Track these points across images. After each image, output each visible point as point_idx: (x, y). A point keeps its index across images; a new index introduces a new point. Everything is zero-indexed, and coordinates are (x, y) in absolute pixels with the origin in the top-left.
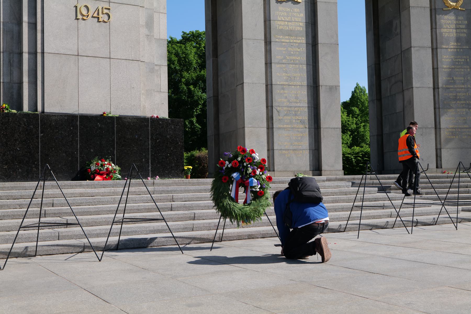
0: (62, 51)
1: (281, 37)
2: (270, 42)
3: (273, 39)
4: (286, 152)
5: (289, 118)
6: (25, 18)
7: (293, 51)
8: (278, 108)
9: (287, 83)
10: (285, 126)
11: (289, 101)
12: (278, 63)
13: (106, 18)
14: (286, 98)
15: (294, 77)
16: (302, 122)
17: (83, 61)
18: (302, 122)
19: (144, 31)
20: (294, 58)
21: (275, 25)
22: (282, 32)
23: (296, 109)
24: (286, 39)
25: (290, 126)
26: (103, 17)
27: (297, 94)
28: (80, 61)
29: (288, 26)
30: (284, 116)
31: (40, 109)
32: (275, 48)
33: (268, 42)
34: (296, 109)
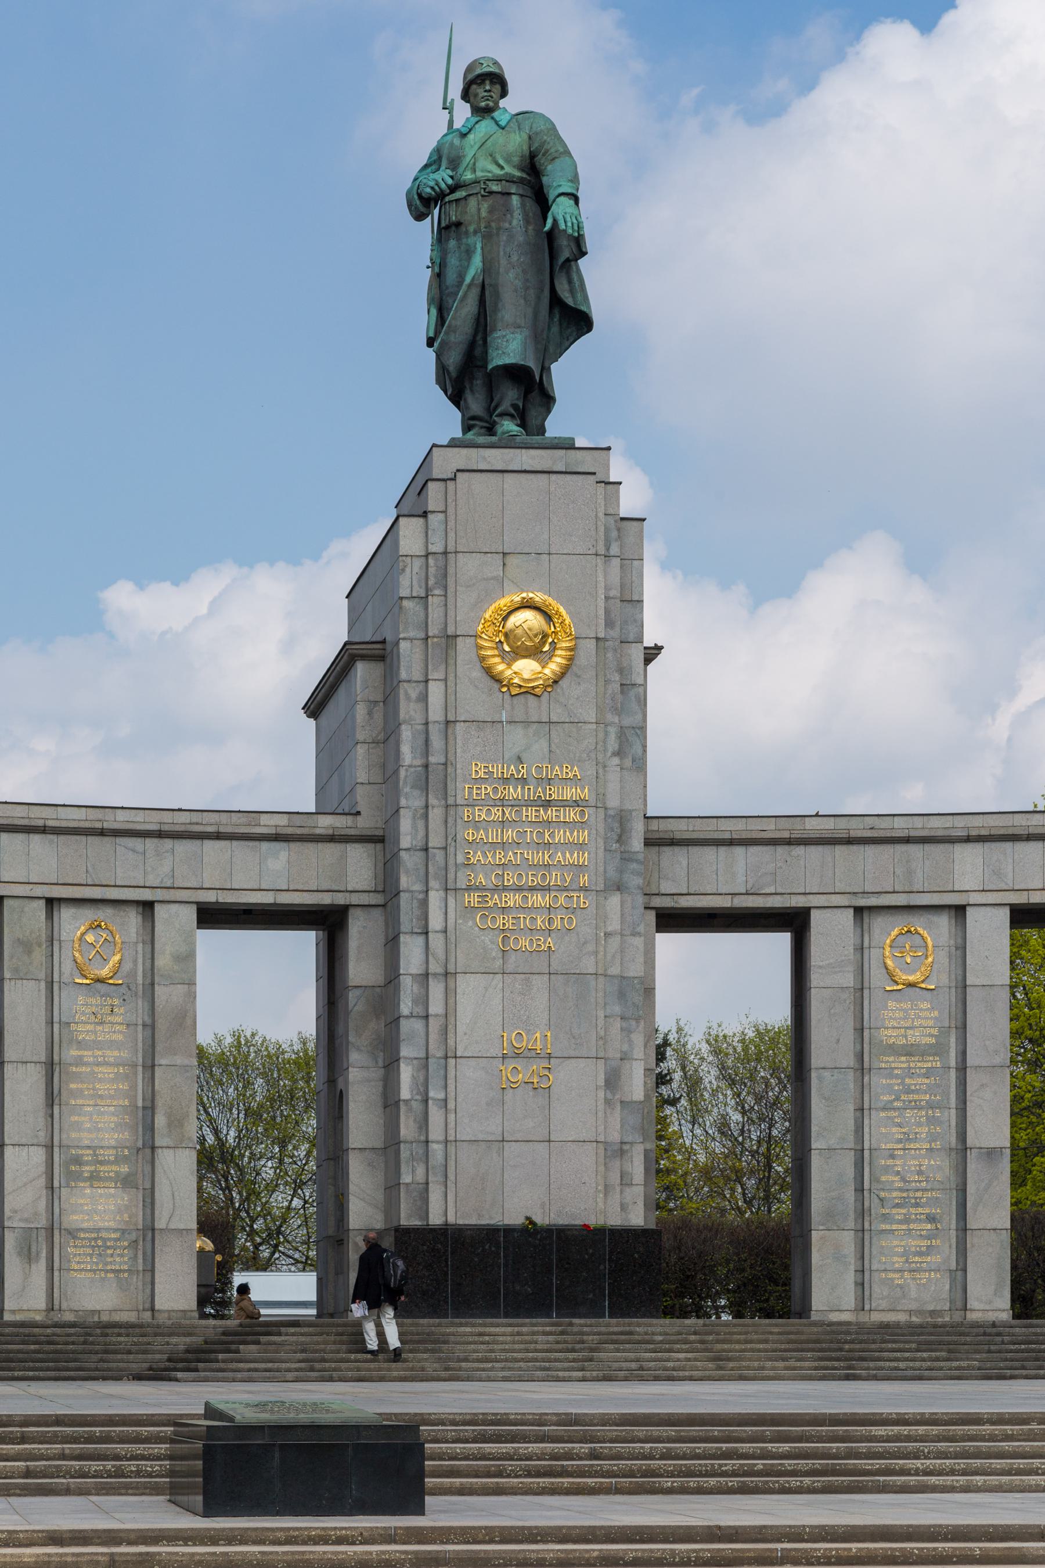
0: (481, 1137)
1: (891, 1059)
4: (897, 1276)
5: (904, 1211)
7: (915, 1085)
8: (882, 1194)
9: (900, 1146)
10: (894, 1227)
12: (884, 1109)
14: (898, 1173)
15: (916, 1133)
16: (931, 1219)
17: (510, 1149)
20: (916, 1097)
22: (894, 1050)
24: (901, 1063)
27: (920, 1165)
28: (506, 1148)
30: (894, 1207)
32: (878, 1081)
33: (861, 1069)
34: (919, 1194)
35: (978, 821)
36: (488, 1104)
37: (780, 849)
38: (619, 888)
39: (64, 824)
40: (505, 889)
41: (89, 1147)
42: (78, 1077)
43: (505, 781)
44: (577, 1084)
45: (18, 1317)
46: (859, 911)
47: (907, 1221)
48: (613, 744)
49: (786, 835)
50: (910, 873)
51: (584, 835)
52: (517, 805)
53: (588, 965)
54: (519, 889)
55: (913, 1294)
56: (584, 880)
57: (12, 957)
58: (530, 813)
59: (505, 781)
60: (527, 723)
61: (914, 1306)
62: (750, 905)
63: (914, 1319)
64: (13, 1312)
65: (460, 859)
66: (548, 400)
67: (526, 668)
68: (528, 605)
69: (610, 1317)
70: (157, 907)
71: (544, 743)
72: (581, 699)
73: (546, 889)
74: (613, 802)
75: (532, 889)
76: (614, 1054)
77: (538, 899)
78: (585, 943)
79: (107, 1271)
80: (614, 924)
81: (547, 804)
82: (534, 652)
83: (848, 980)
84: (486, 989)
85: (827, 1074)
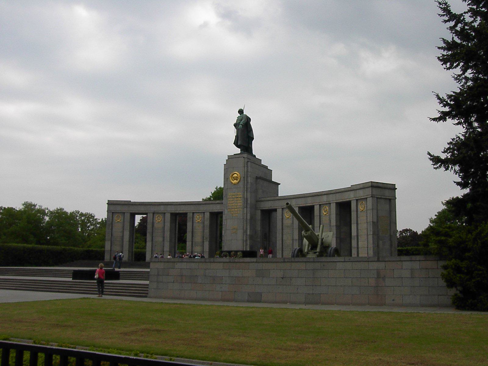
16: (290, 249)
38: (247, 207)
40: (232, 209)
43: (233, 195)
44: (240, 233)
48: (245, 190)
51: (241, 201)
52: (234, 198)
54: (234, 208)
56: (241, 207)
58: (235, 199)
59: (233, 195)
60: (235, 188)
67: (235, 181)
68: (235, 174)
70: (205, 213)
72: (241, 184)
73: (237, 208)
74: (245, 197)
75: (236, 208)
76: (245, 228)
77: (236, 210)
80: (245, 212)
81: (237, 198)
82: (236, 179)
83: (281, 218)
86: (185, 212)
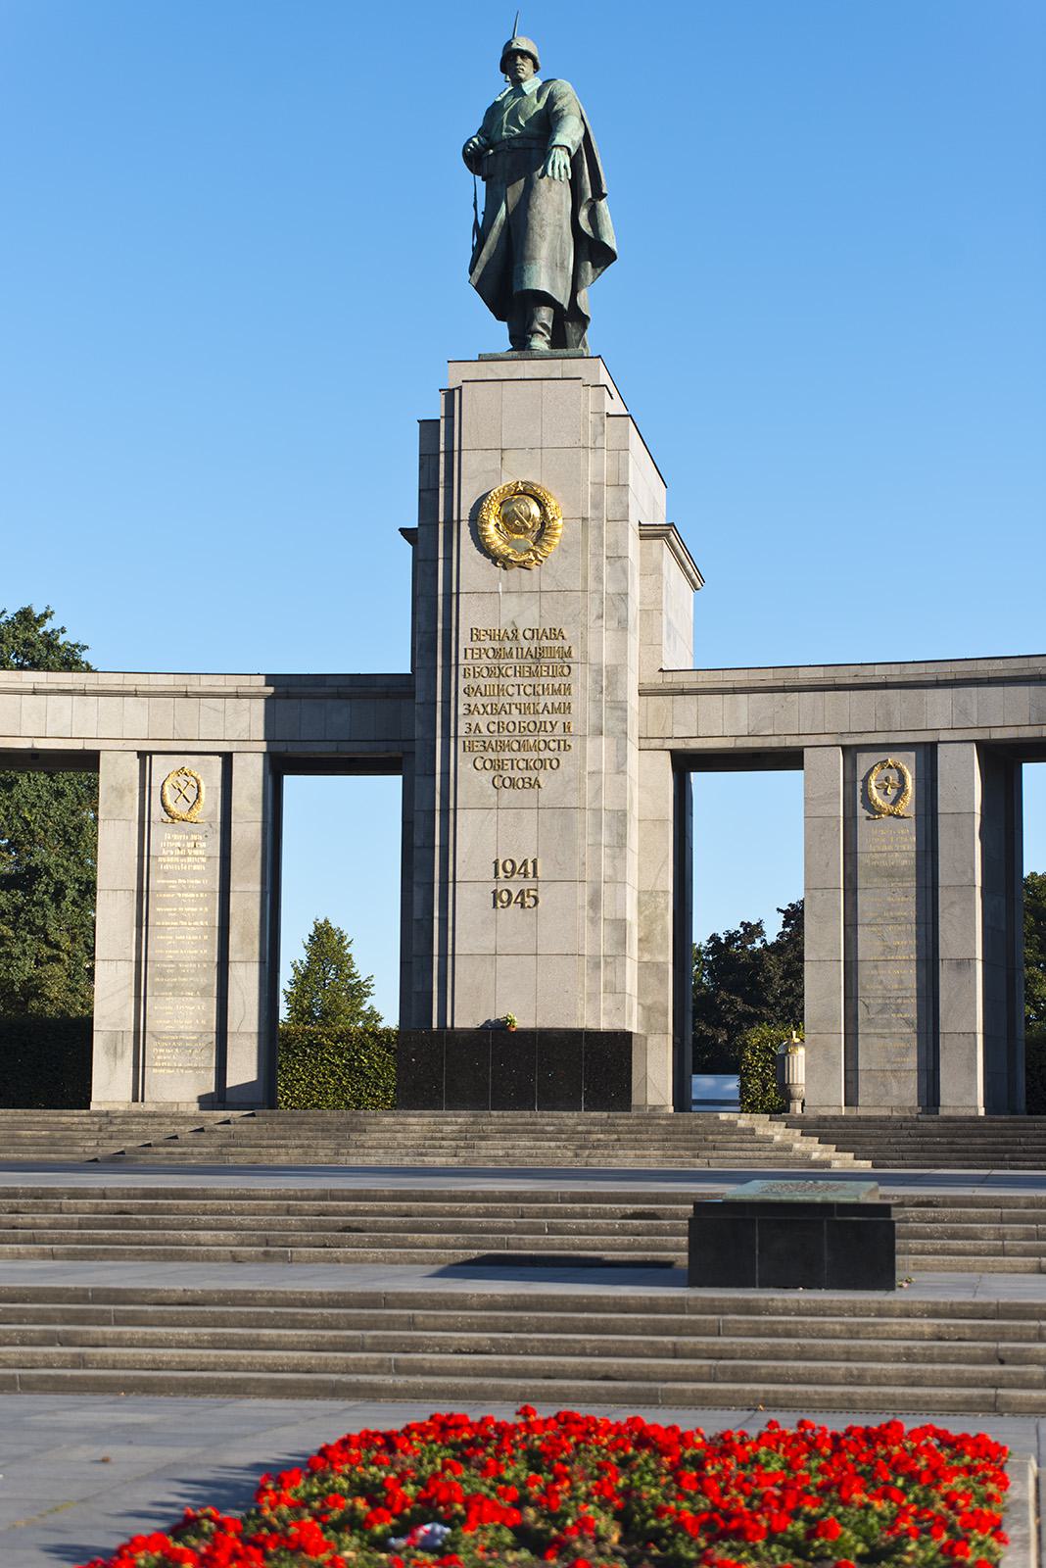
2: (856, 890)
3: (861, 883)
6: (436, 914)
8: (867, 1002)
11: (885, 988)
13: (530, 902)
15: (897, 946)
16: (908, 1022)
17: (502, 961)
18: (908, 1022)
19: (587, 912)
21: (862, 859)
22: (878, 871)
23: (899, 1001)
25: (886, 1031)
26: (530, 902)
29: (886, 859)
31: (449, 1024)
32: (862, 899)
35: (948, 667)
36: (483, 923)
37: (777, 695)
39: (152, 689)
41: (172, 962)
42: (164, 902)
45: (104, 1108)
46: (846, 749)
47: (889, 1024)
49: (780, 683)
50: (889, 715)
53: (572, 800)
55: (895, 1092)
57: (105, 802)
60: (520, 593)
61: (895, 1103)
62: (751, 745)
63: (895, 1114)
64: (99, 1103)
65: (462, 710)
66: (583, 320)
69: (585, 1110)
71: (535, 610)
78: (569, 781)
79: (186, 1068)
84: (482, 822)
85: (818, 894)
86: (77, 745)
